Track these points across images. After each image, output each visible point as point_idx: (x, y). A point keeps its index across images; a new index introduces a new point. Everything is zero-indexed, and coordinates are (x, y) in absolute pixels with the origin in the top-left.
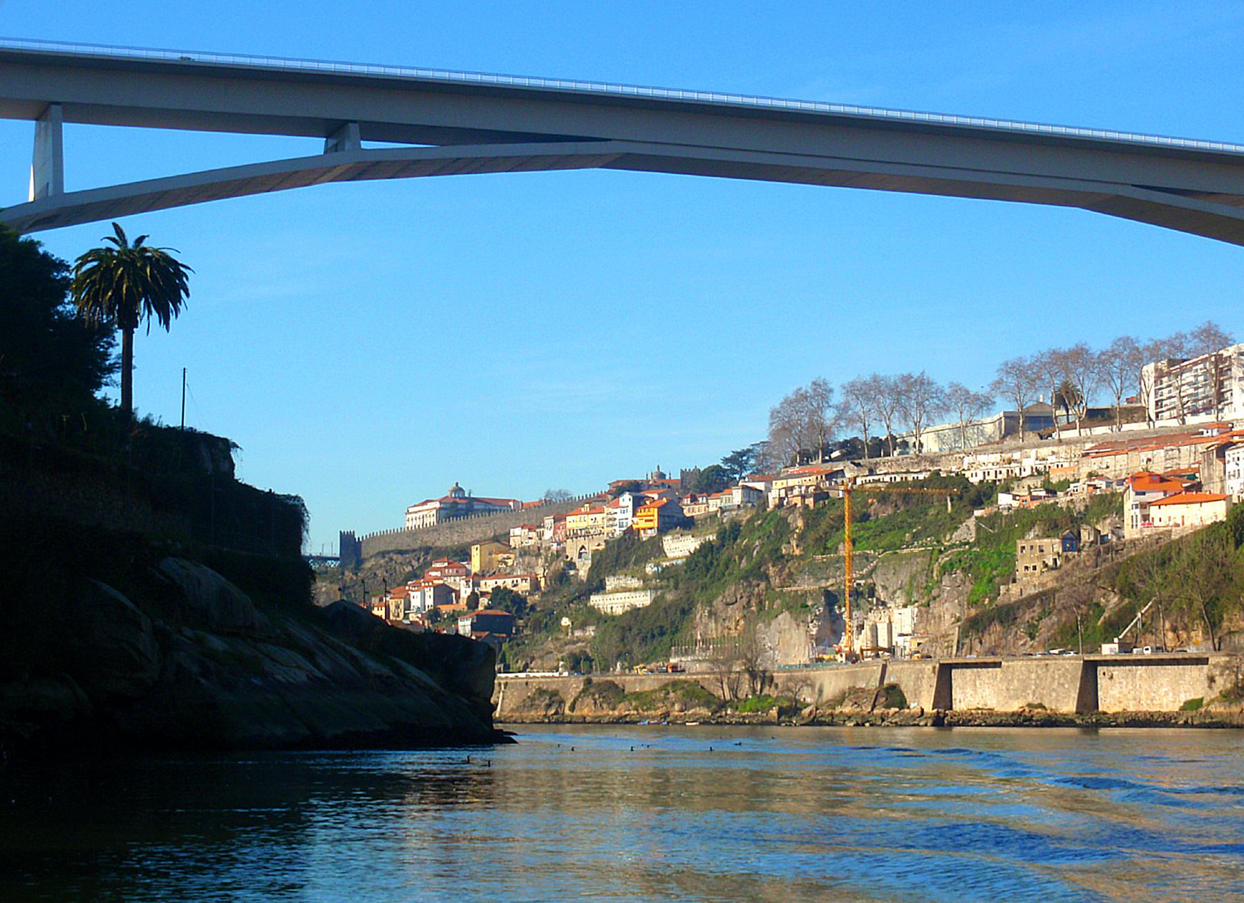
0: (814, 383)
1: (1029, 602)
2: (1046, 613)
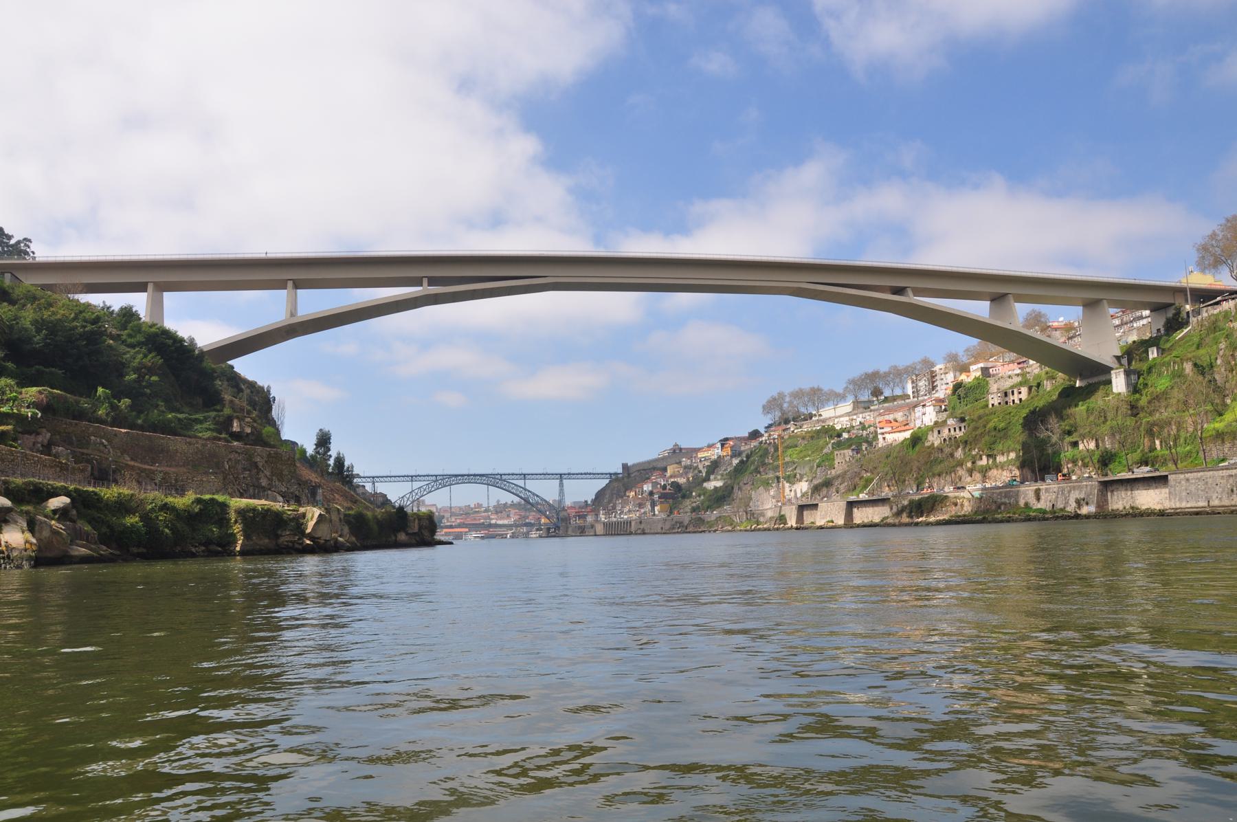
0: (779, 393)
1: (838, 476)
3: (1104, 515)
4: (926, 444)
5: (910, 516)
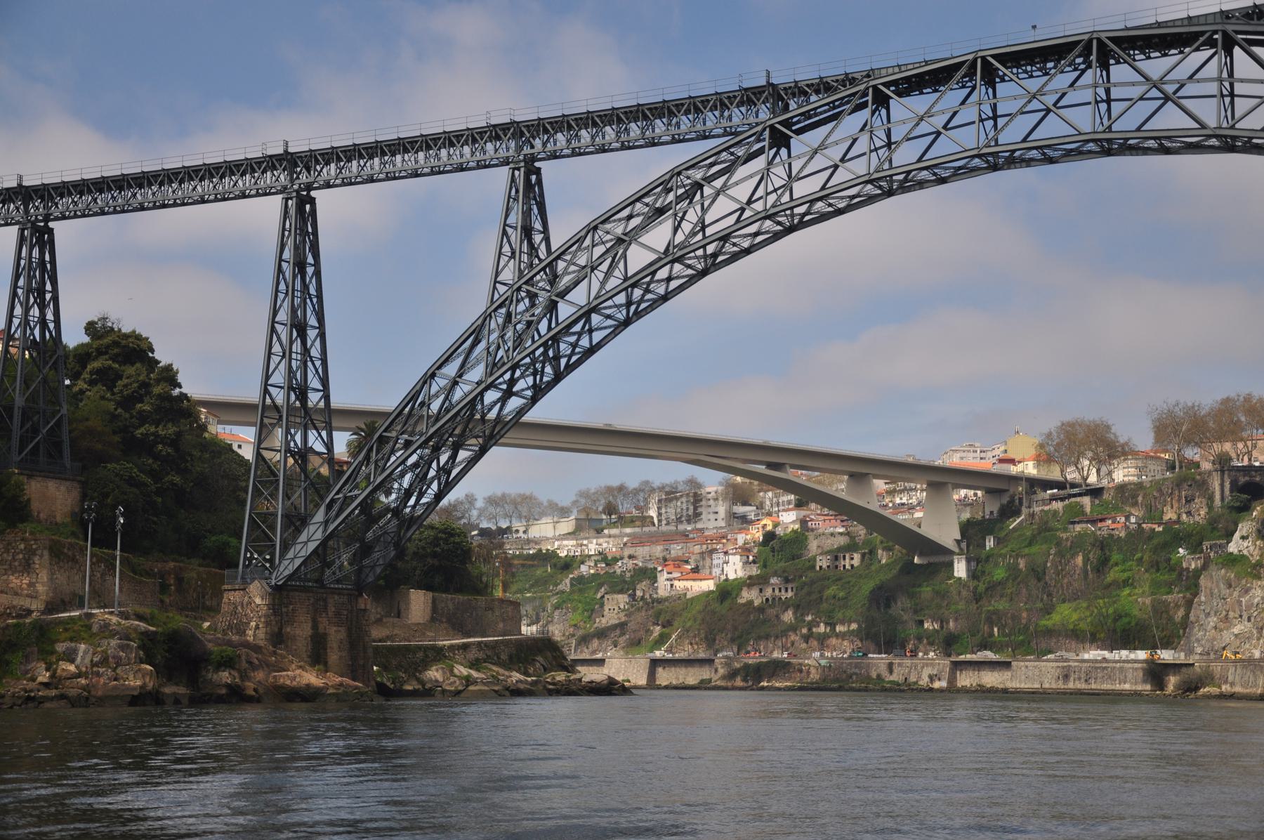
1: (614, 627)
2: (623, 634)
3: (953, 691)
4: (741, 601)
5: (745, 680)
